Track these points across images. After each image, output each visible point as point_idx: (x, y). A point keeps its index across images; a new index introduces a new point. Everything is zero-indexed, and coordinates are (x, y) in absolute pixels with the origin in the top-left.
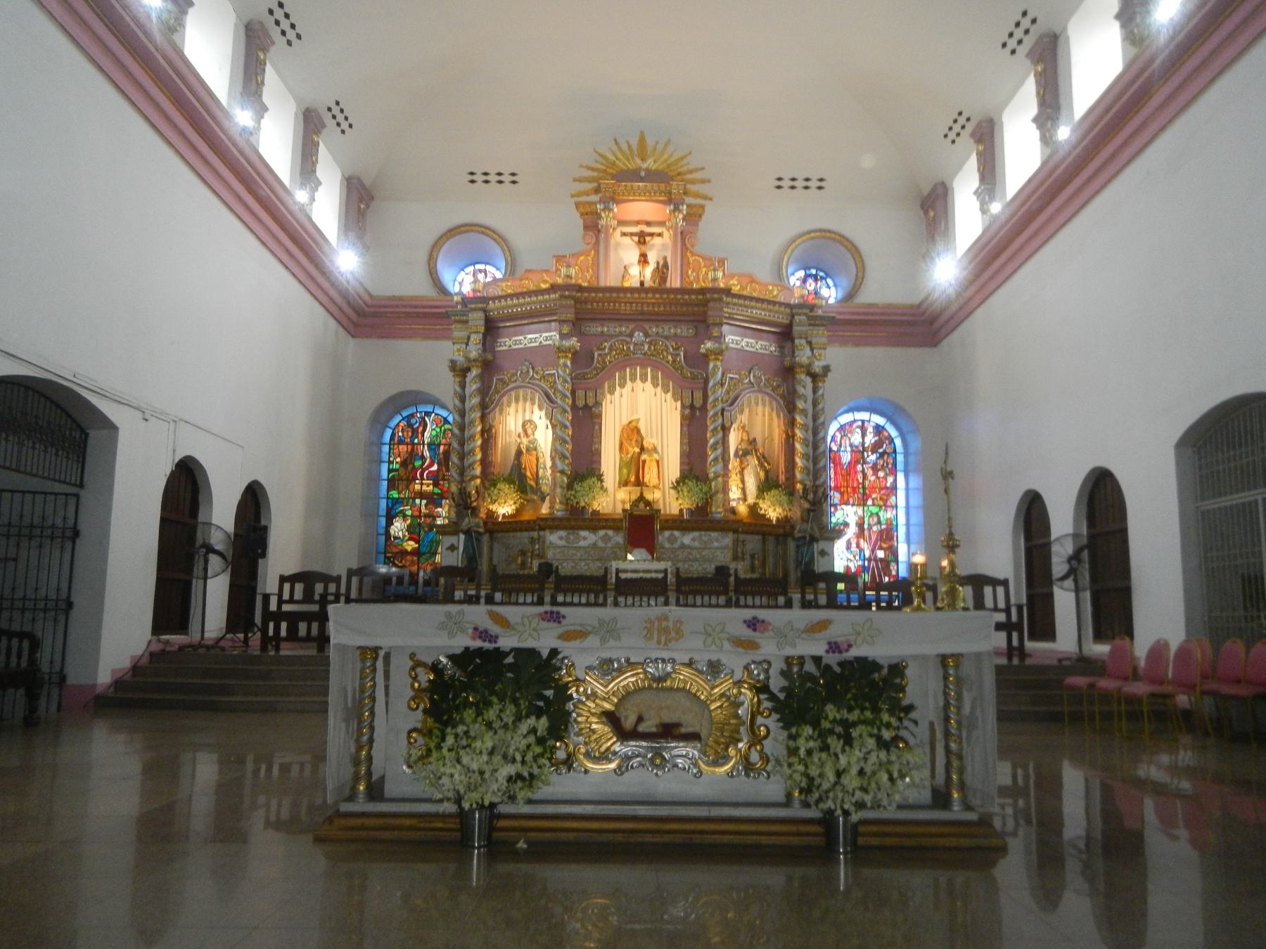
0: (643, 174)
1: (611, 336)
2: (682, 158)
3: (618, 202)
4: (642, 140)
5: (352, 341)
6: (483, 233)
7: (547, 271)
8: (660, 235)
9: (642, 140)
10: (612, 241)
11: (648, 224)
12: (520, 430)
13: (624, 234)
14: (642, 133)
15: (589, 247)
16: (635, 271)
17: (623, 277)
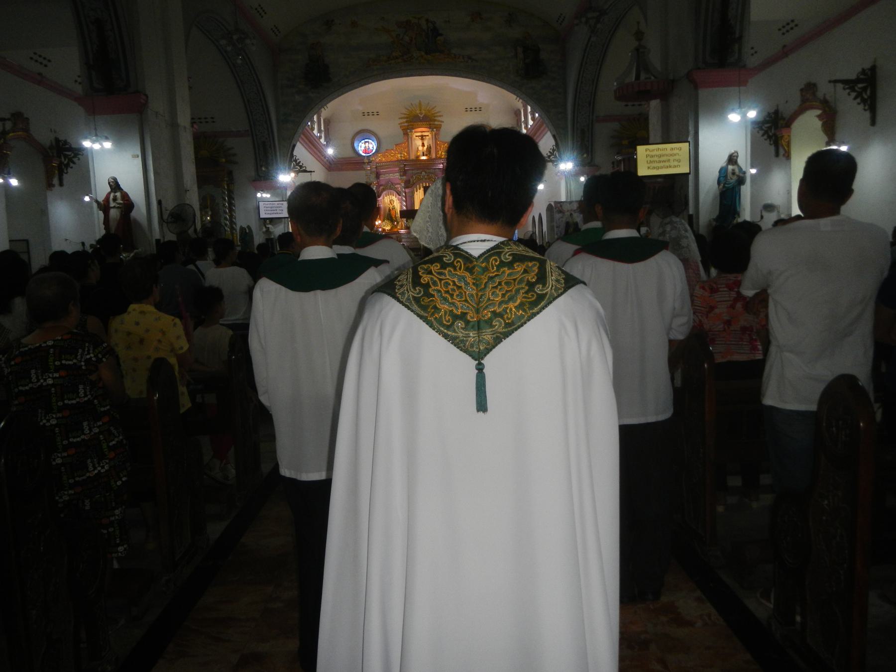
0: (421, 119)
1: (415, 174)
2: (433, 108)
3: (413, 129)
4: (420, 104)
5: (330, 172)
6: (369, 132)
7: (393, 150)
8: (428, 136)
9: (420, 104)
10: (413, 138)
11: (424, 132)
12: (389, 202)
13: (416, 136)
14: (420, 101)
15: (405, 141)
16: (420, 148)
17: (417, 151)
